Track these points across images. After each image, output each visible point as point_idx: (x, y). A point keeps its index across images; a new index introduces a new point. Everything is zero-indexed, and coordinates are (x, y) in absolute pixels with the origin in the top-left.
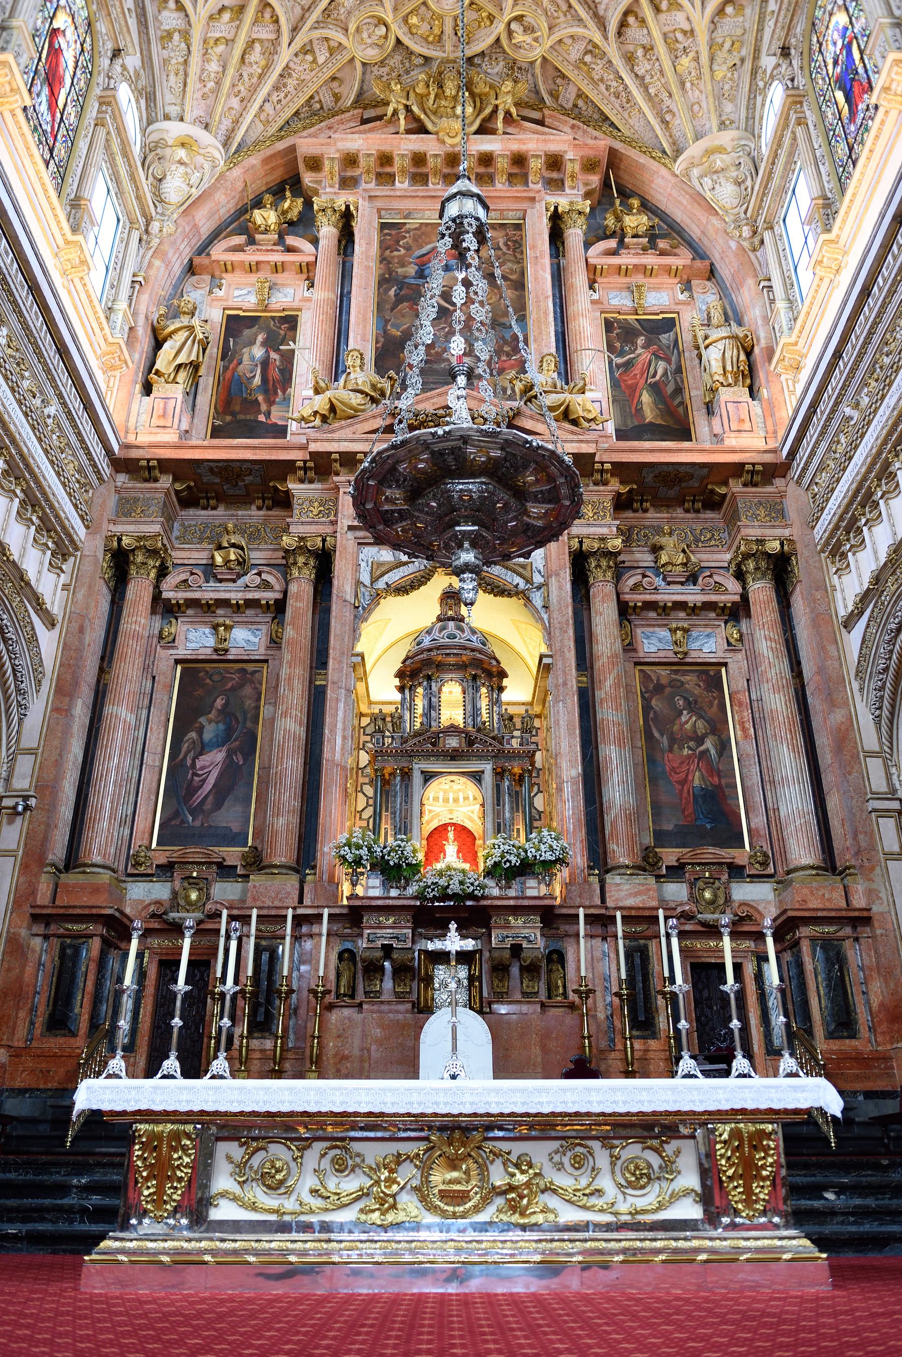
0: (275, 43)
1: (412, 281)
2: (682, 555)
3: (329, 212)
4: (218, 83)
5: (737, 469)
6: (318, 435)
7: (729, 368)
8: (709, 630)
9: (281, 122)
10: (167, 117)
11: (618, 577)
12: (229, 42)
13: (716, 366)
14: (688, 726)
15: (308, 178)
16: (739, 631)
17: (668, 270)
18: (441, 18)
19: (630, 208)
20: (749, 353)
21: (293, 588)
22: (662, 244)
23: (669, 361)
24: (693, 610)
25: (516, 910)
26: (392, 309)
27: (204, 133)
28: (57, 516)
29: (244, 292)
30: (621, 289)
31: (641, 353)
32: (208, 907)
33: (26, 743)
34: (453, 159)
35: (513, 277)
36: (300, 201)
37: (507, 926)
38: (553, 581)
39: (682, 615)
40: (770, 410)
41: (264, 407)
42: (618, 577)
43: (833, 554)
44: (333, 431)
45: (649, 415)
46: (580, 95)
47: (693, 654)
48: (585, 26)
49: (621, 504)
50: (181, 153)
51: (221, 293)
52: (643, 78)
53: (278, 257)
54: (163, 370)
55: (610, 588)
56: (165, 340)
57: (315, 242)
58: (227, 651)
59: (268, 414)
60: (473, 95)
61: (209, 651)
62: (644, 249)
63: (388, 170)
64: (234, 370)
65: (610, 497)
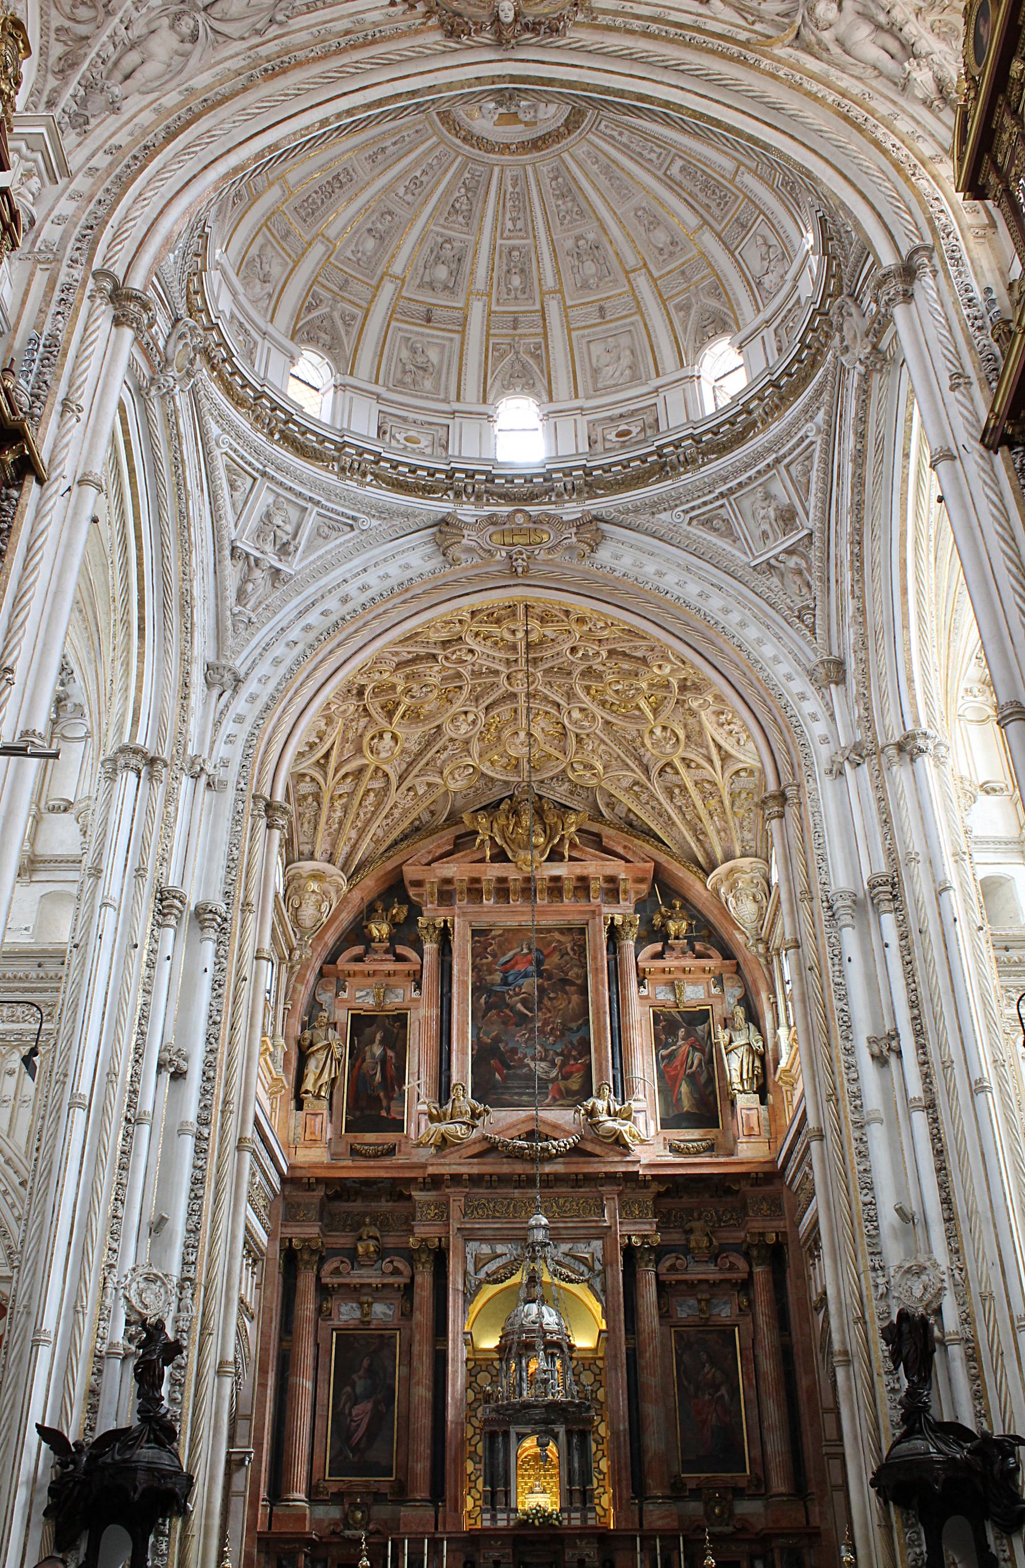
0: (386, 789)
1: (498, 989)
2: (706, 1239)
3: (431, 930)
4: (341, 823)
5: (746, 1175)
6: (434, 1161)
7: (745, 1076)
8: (726, 1298)
9: (388, 842)
10: (301, 855)
11: (657, 1263)
12: (351, 795)
13: (736, 1079)
14: (710, 1376)
15: (412, 892)
16: (749, 1301)
17: (704, 970)
18: (517, 759)
19: (673, 907)
20: (762, 1057)
21: (419, 1279)
22: (698, 946)
23: (702, 1051)
24: (714, 1284)
25: (581, 1536)
26: (483, 1017)
27: (330, 866)
28: (256, 1244)
29: (363, 993)
30: (666, 984)
31: (682, 1045)
32: (371, 1527)
33: (241, 1411)
34: (528, 880)
35: (579, 982)
36: (405, 909)
37: (574, 1546)
38: (609, 1269)
39: (705, 1287)
40: (774, 1115)
41: (384, 1103)
42: (657, 1263)
43: (810, 1249)
44: (444, 1157)
45: (686, 1105)
46: (630, 810)
47: (713, 1318)
48: (633, 770)
49: (659, 1195)
50: (313, 886)
51: (344, 995)
52: (680, 807)
53: (390, 966)
54: (310, 1088)
55: (651, 1276)
56: (309, 1056)
57: (417, 946)
58: (369, 1322)
59: (388, 1111)
60: (544, 824)
61: (357, 1322)
62: (684, 953)
63: (477, 886)
64: (360, 1067)
65: (652, 1196)
